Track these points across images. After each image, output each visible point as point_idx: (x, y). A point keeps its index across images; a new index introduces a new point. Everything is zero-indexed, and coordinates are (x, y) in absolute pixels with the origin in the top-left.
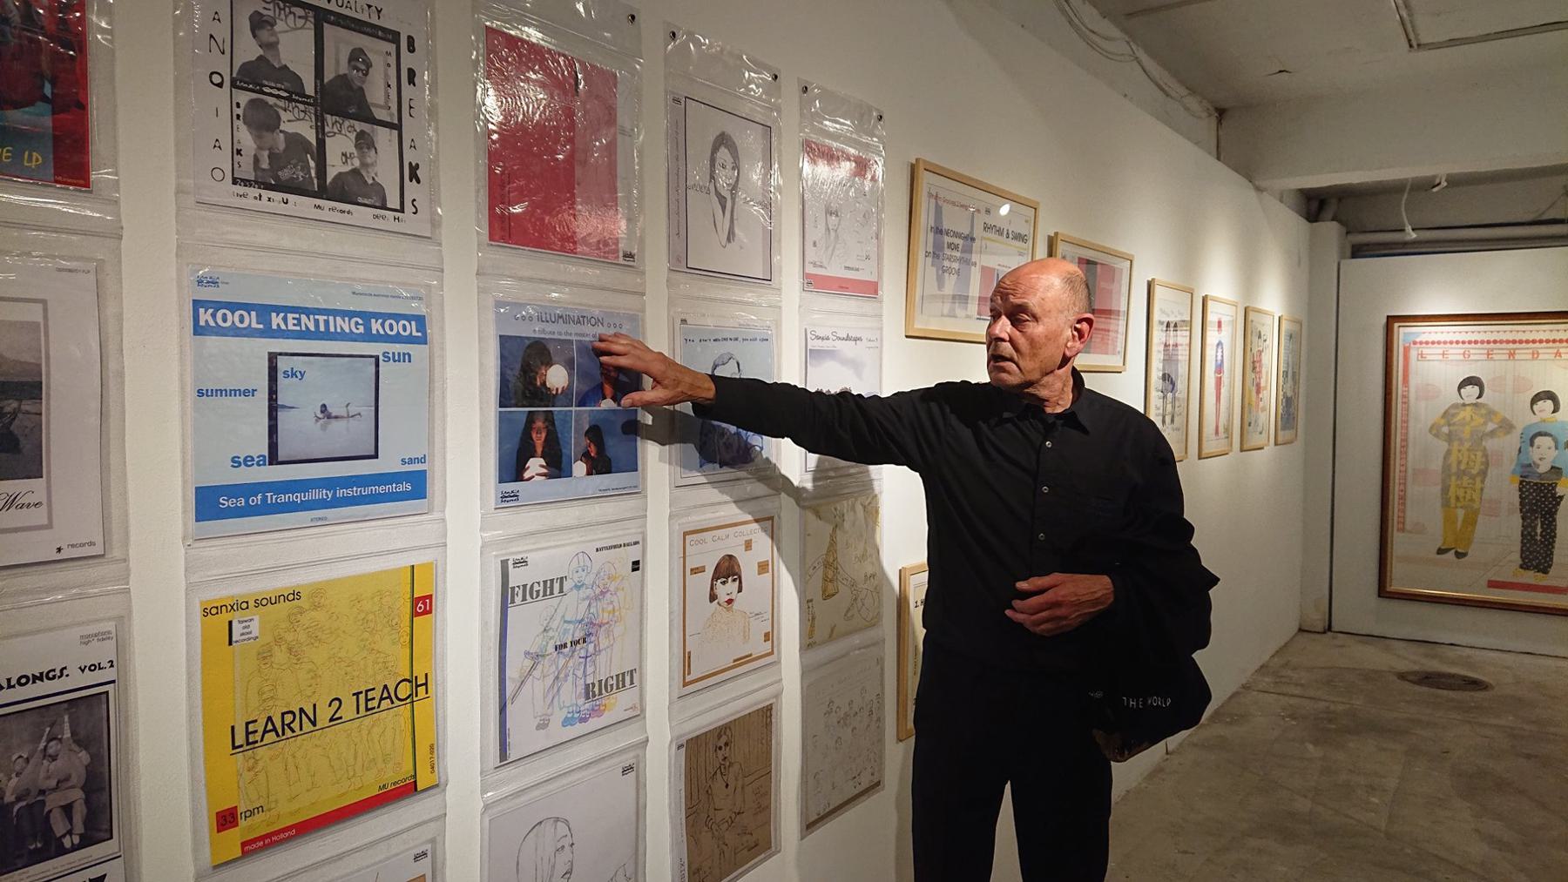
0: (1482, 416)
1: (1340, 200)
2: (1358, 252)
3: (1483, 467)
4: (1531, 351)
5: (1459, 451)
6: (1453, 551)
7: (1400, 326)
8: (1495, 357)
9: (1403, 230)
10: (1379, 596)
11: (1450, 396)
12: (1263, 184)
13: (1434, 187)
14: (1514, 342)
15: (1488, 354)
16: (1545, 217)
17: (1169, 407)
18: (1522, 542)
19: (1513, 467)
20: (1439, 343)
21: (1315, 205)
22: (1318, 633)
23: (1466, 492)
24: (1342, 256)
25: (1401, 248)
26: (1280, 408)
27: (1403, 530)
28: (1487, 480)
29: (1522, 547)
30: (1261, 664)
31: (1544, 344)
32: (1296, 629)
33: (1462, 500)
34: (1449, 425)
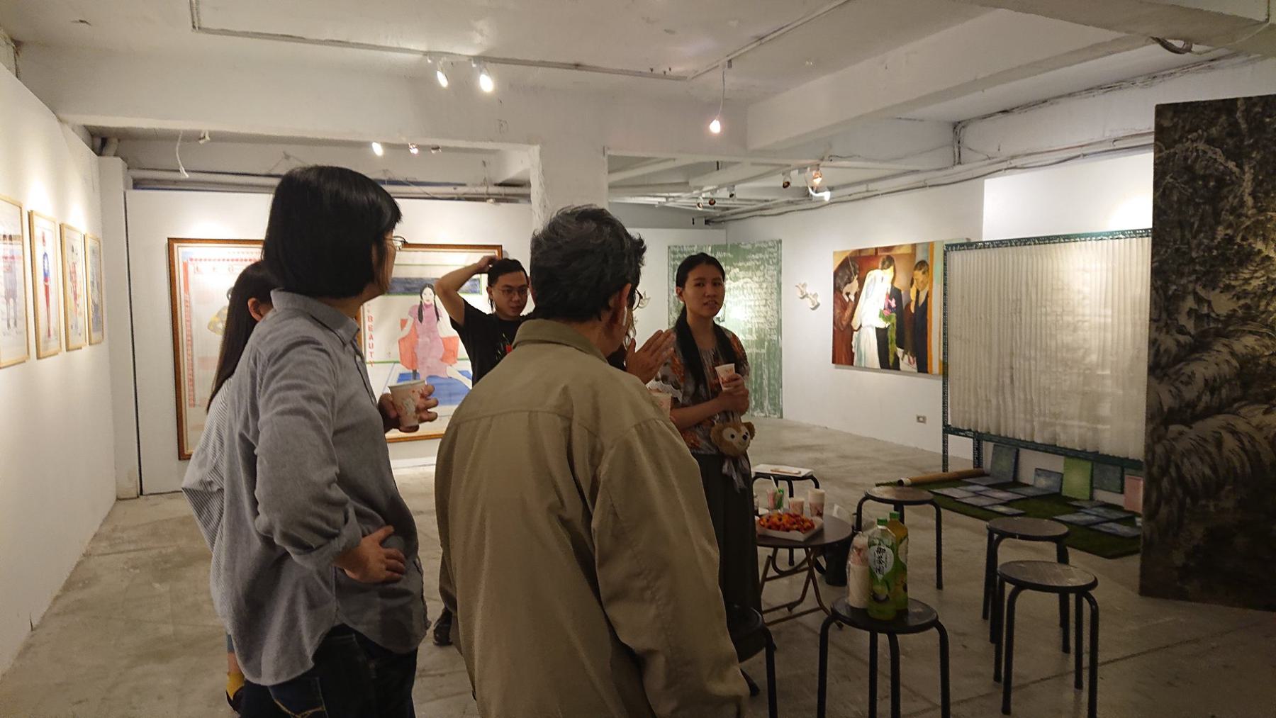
1: (119, 140)
2: (138, 184)
7: (178, 247)
9: (179, 171)
10: (180, 459)
12: (64, 116)
13: (200, 139)
17: (12, 314)
21: (100, 141)
22: (132, 499)
24: (127, 187)
25: (173, 185)
26: (91, 312)
27: (194, 405)
30: (93, 534)
32: (115, 499)
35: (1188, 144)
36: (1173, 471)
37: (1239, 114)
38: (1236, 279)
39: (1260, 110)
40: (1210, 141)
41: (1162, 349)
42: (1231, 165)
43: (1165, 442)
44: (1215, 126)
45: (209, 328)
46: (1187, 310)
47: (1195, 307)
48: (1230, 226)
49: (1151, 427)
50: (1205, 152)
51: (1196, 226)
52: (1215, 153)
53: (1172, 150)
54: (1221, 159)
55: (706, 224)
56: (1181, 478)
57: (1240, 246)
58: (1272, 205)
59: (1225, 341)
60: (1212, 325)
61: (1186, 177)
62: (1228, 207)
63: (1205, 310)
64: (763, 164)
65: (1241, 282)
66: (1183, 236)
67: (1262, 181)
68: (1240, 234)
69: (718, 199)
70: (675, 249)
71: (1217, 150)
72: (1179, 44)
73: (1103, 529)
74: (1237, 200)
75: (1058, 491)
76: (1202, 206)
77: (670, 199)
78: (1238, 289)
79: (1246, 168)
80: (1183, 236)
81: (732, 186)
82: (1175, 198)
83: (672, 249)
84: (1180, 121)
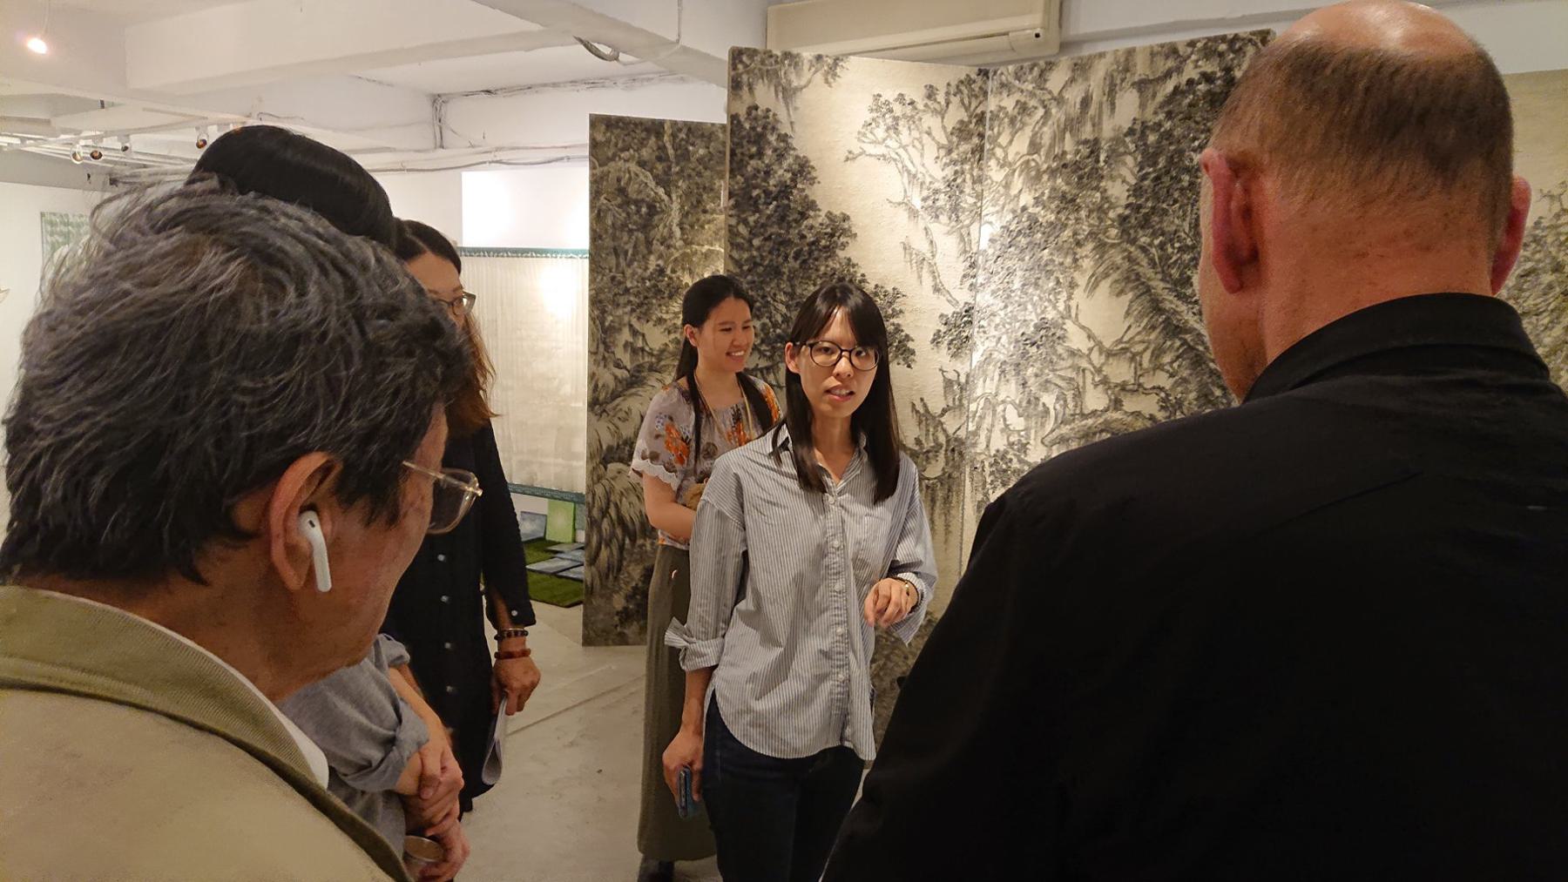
35: (621, 163)
36: (612, 512)
37: (666, 138)
38: (667, 312)
39: (684, 137)
40: (642, 164)
41: (600, 385)
42: (661, 191)
43: (604, 481)
44: (645, 146)
46: (623, 342)
47: (631, 340)
48: (660, 257)
49: (591, 468)
50: (637, 175)
51: (630, 252)
52: (646, 177)
53: (605, 168)
54: (652, 184)
55: (111, 184)
56: (621, 520)
57: (670, 278)
58: (696, 239)
59: (658, 375)
60: (646, 359)
61: (619, 200)
62: (658, 237)
63: (640, 344)
64: (175, 114)
65: (672, 316)
66: (618, 265)
67: (687, 213)
68: (670, 266)
69: (106, 149)
70: (53, 218)
71: (649, 174)
72: (606, 50)
73: (571, 576)
74: (666, 229)
75: (542, 535)
76: (636, 233)
77: (28, 142)
78: (669, 323)
79: (674, 198)
80: (618, 265)
81: (125, 135)
82: (610, 223)
83: (48, 217)
84: (613, 137)
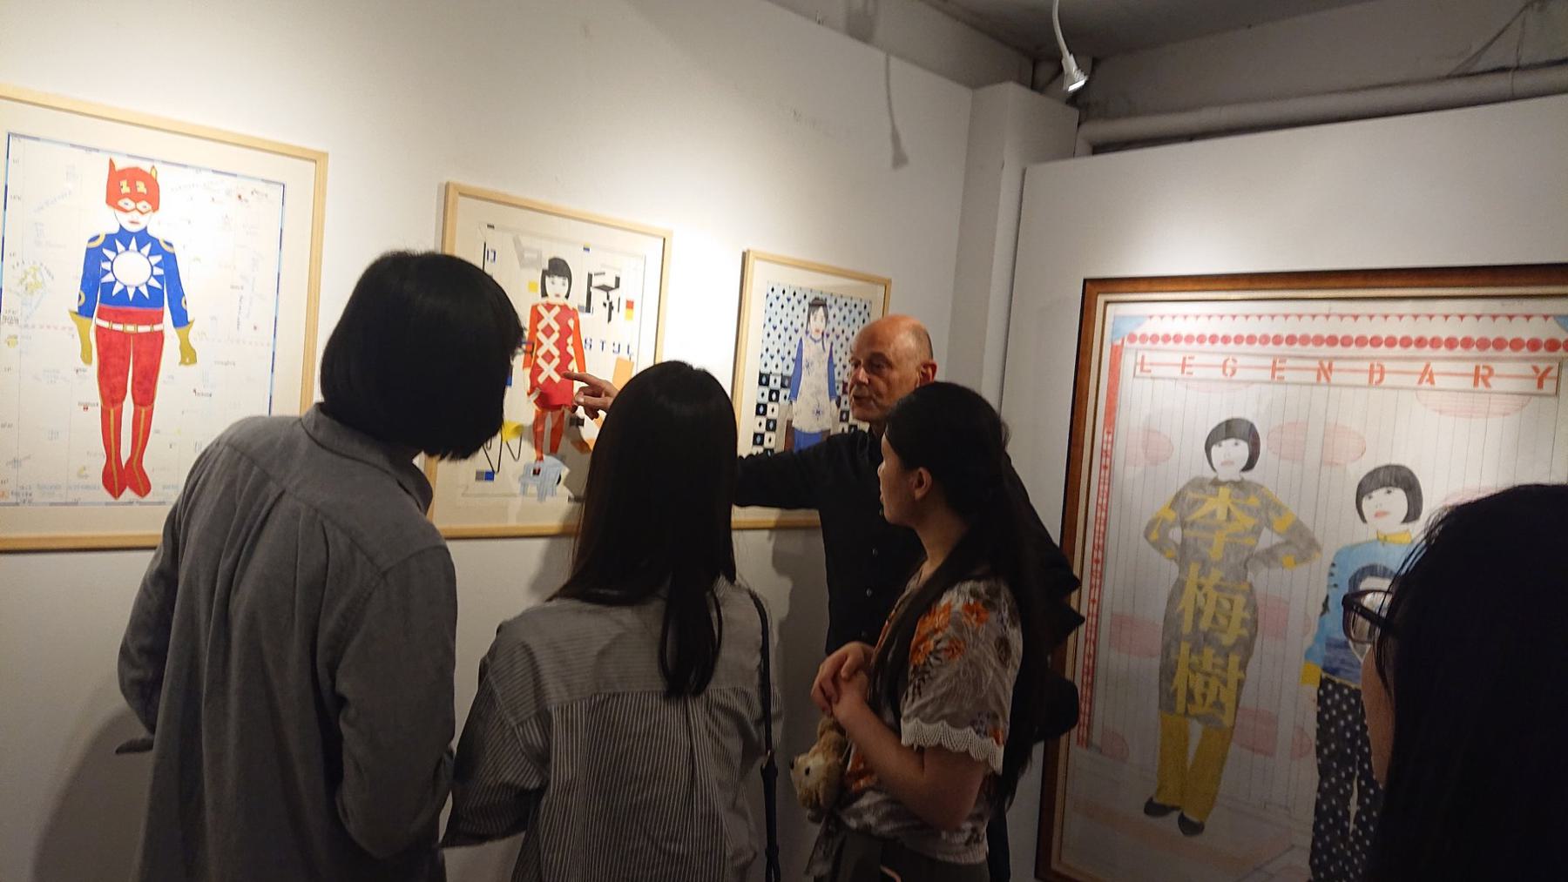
0: (1249, 511)
3: (1245, 632)
4: (1366, 365)
5: (1200, 587)
6: (1175, 815)
7: (1107, 303)
8: (1288, 376)
11: (1189, 461)
14: (1332, 341)
15: (1274, 369)
16: (1480, 66)
18: (1316, 827)
19: (1308, 641)
20: (1177, 339)
23: (1206, 684)
28: (1253, 663)
29: (1314, 841)
31: (1397, 350)
33: (1198, 698)
34: (1184, 525)
45: (1146, 536)
